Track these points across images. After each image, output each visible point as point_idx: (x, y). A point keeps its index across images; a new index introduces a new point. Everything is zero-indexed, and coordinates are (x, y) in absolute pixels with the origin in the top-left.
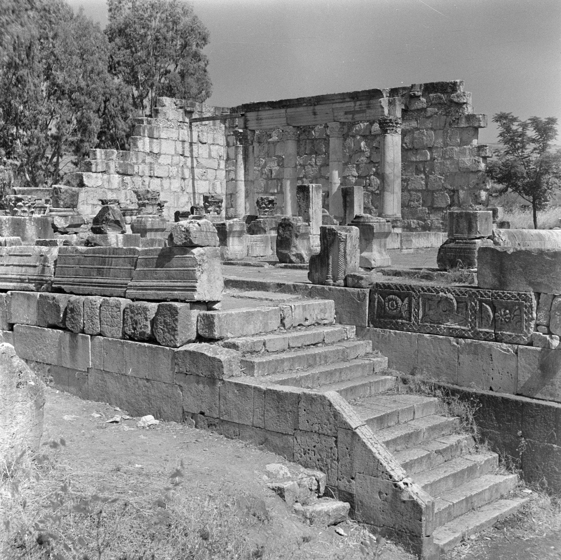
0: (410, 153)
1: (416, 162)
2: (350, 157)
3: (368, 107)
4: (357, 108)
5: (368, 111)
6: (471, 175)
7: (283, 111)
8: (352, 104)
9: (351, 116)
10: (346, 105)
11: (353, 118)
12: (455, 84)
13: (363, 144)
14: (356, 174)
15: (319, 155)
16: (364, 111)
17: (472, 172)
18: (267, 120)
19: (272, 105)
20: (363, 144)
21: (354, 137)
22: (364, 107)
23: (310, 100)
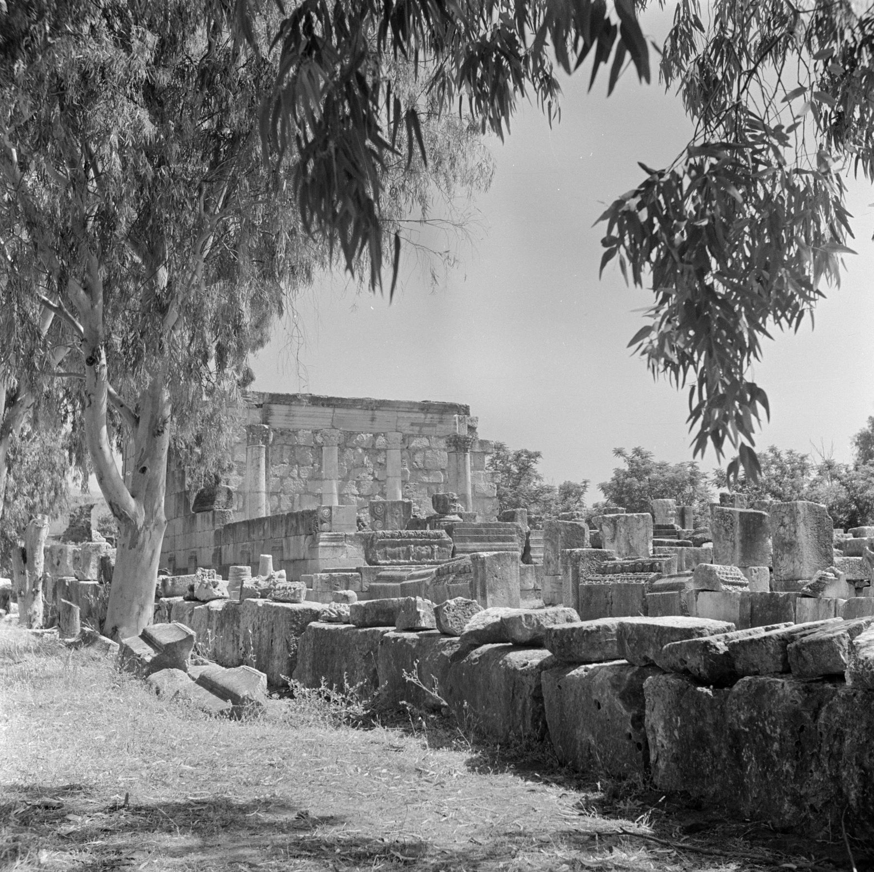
0: (419, 473)
1: (428, 483)
2: (349, 471)
3: (441, 422)
4: (428, 421)
5: (439, 426)
6: (487, 501)
7: (329, 410)
8: (423, 416)
9: (417, 428)
10: (413, 415)
11: (420, 431)
12: (467, 407)
13: (366, 458)
14: (357, 493)
15: (303, 466)
16: (434, 426)
17: (488, 498)
18: (301, 418)
19: (315, 401)
20: (366, 458)
21: (354, 448)
22: (436, 421)
23: (371, 403)
